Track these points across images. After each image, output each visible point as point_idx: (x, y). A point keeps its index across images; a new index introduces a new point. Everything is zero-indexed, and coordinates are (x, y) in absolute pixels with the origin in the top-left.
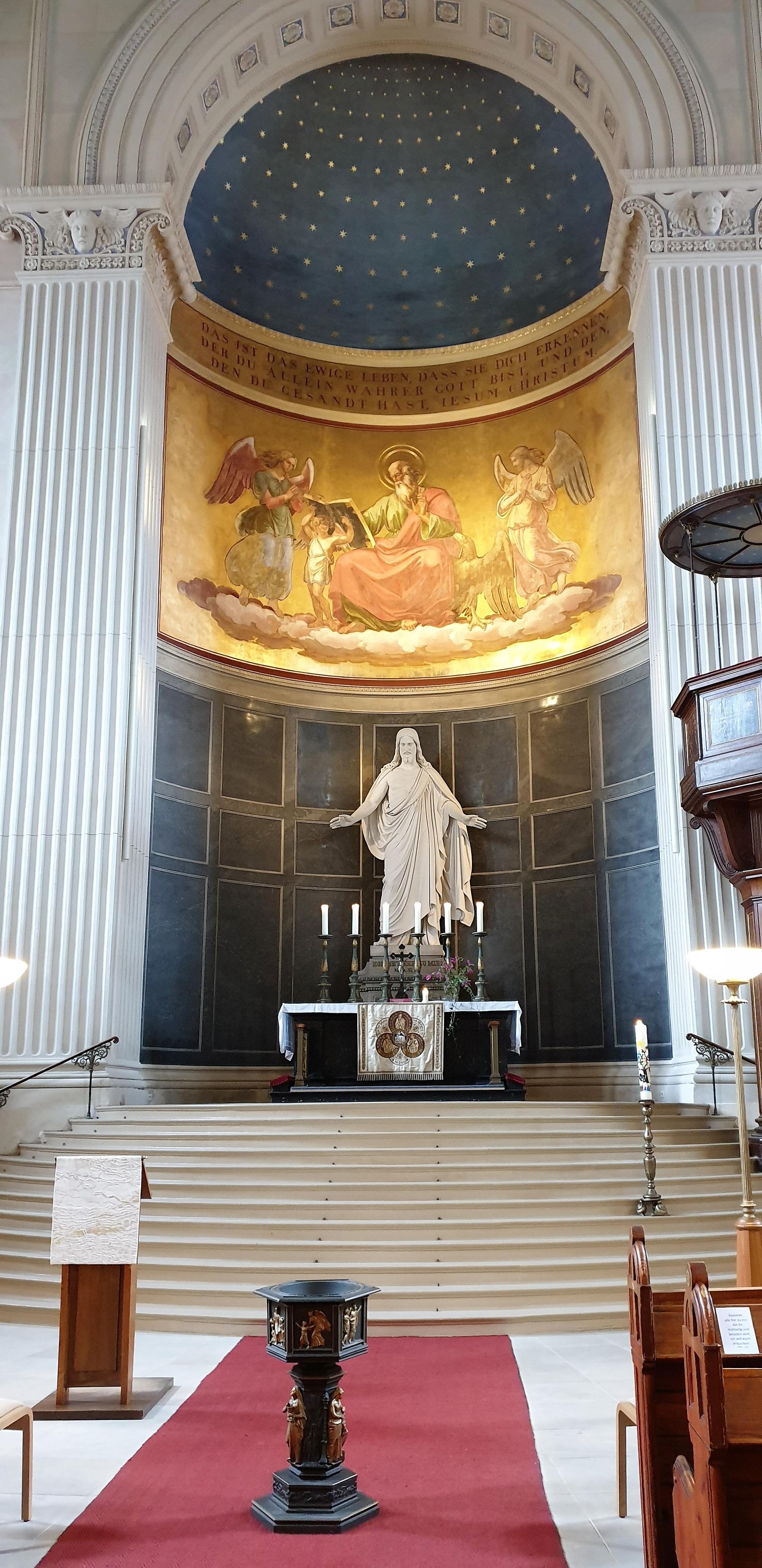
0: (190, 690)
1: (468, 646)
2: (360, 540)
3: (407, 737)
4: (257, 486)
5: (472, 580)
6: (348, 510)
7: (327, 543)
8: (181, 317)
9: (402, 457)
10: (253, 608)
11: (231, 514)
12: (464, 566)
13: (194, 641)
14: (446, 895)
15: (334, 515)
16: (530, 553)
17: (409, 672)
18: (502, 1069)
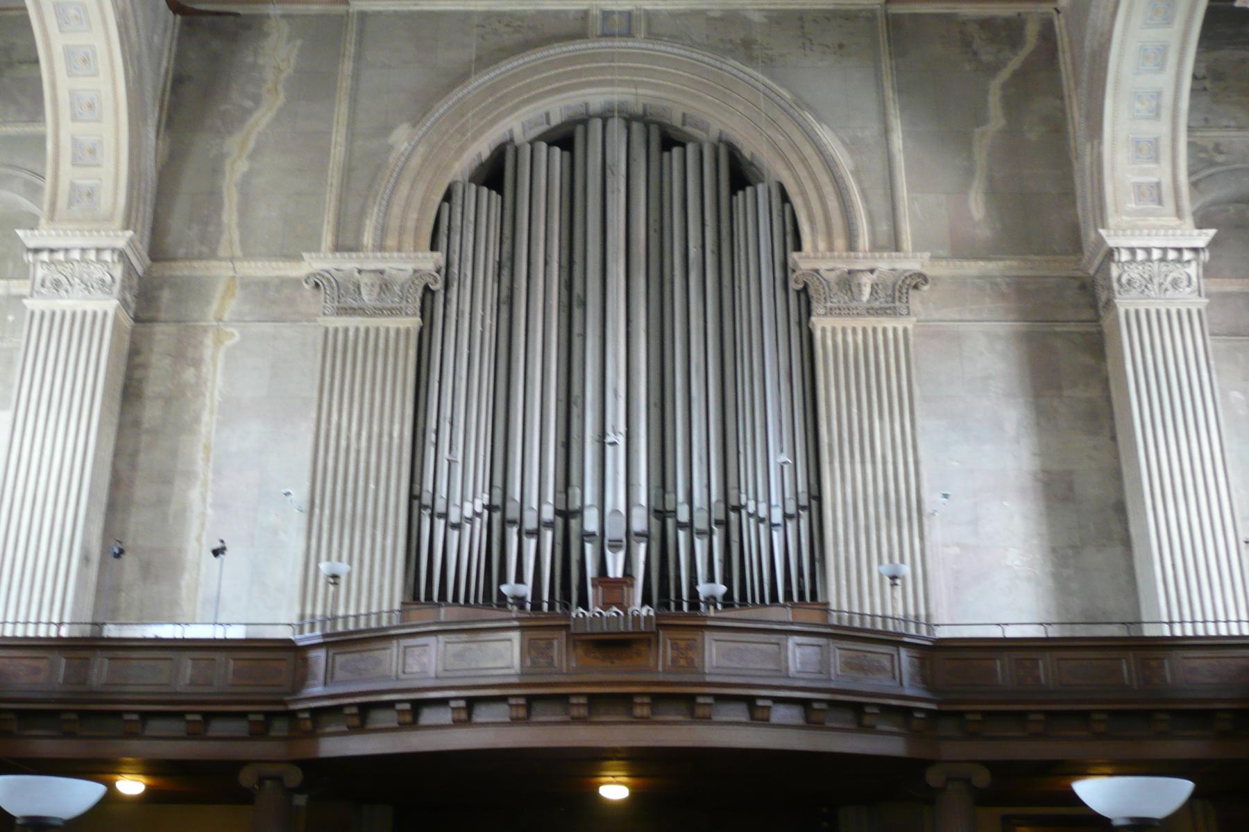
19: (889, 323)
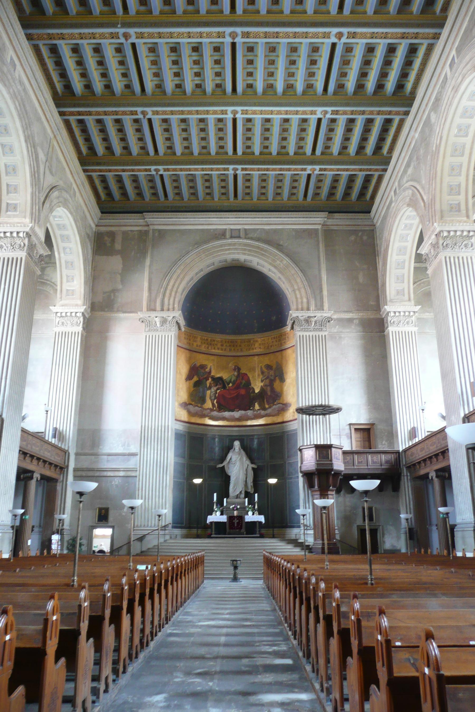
0: (182, 432)
1: (253, 417)
2: (224, 387)
6: (221, 379)
7: (215, 388)
10: (197, 408)
12: (252, 395)
13: (183, 419)
18: (259, 531)
19: (320, 333)
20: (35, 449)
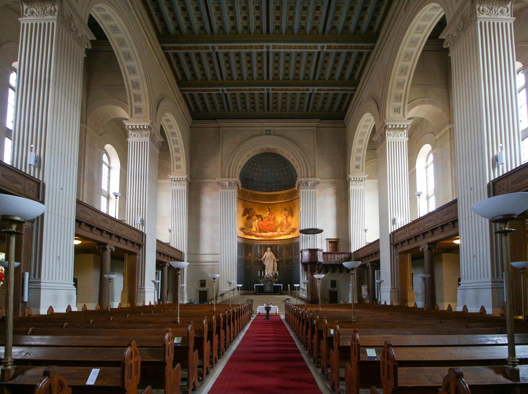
3: (269, 248)
4: (248, 213)
5: (278, 226)
6: (260, 216)
8: (239, 192)
9: (268, 208)
11: (245, 217)
14: (274, 270)
15: (259, 216)
16: (285, 223)
17: (269, 239)
20: (166, 251)
